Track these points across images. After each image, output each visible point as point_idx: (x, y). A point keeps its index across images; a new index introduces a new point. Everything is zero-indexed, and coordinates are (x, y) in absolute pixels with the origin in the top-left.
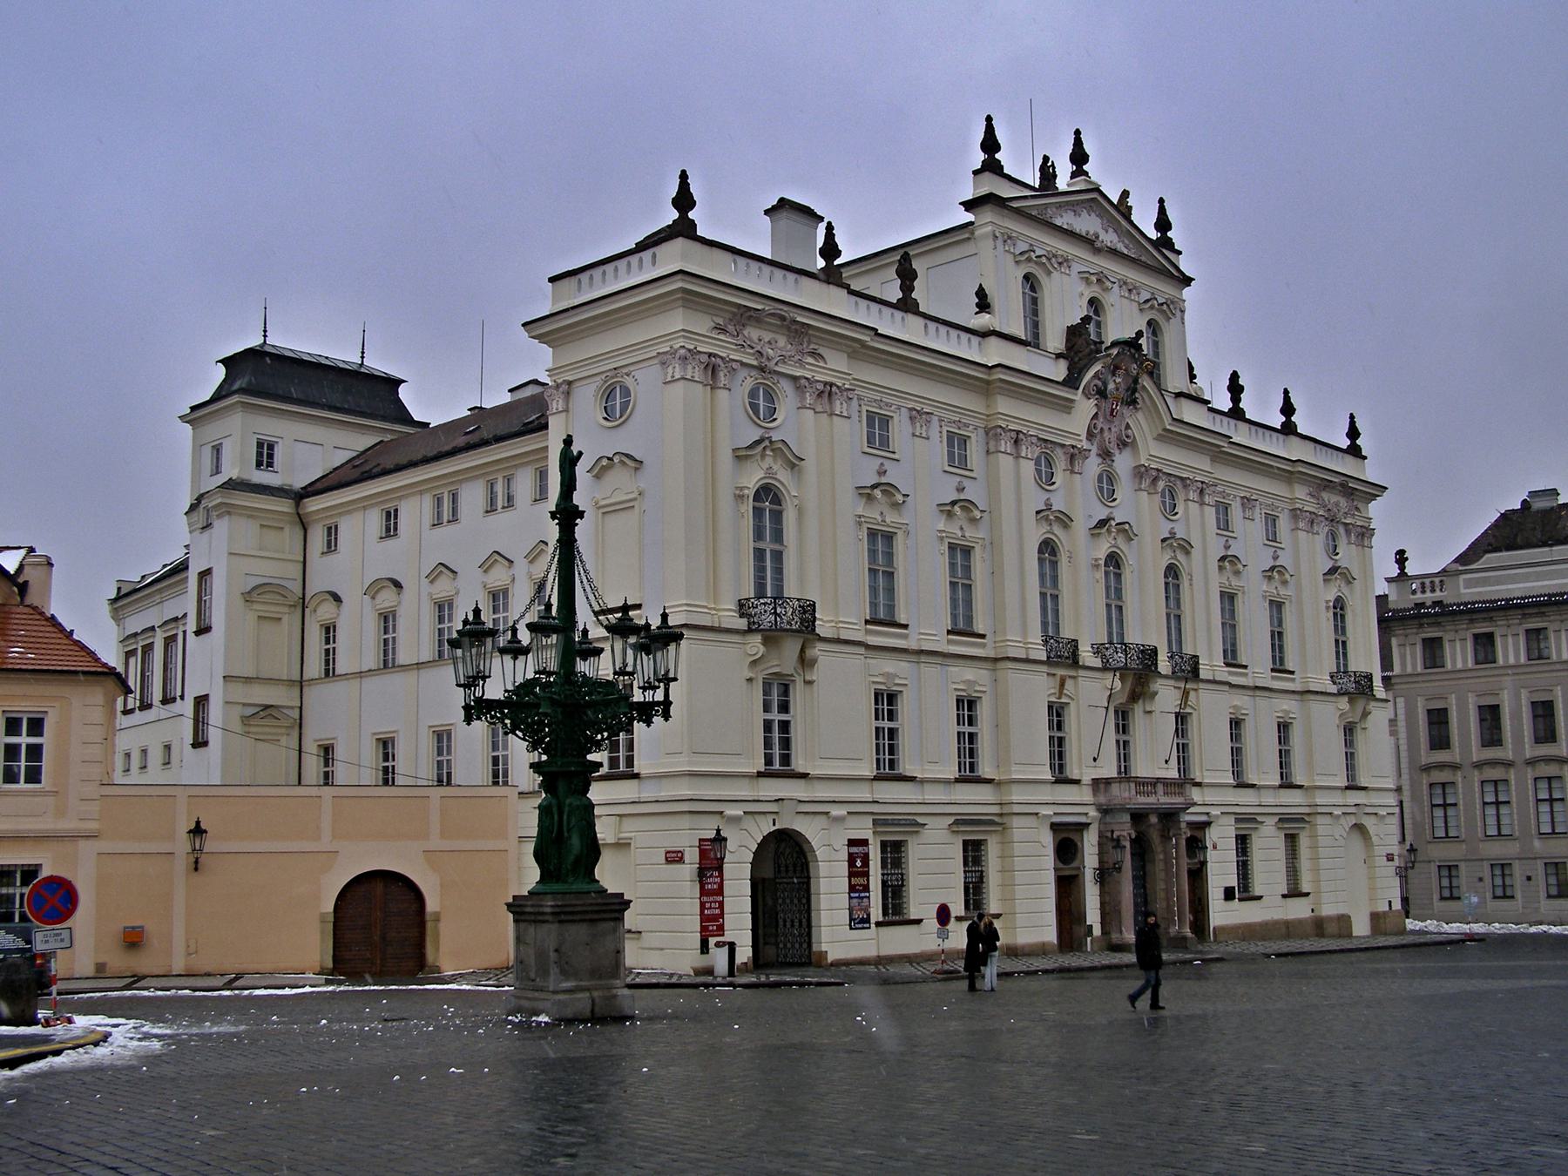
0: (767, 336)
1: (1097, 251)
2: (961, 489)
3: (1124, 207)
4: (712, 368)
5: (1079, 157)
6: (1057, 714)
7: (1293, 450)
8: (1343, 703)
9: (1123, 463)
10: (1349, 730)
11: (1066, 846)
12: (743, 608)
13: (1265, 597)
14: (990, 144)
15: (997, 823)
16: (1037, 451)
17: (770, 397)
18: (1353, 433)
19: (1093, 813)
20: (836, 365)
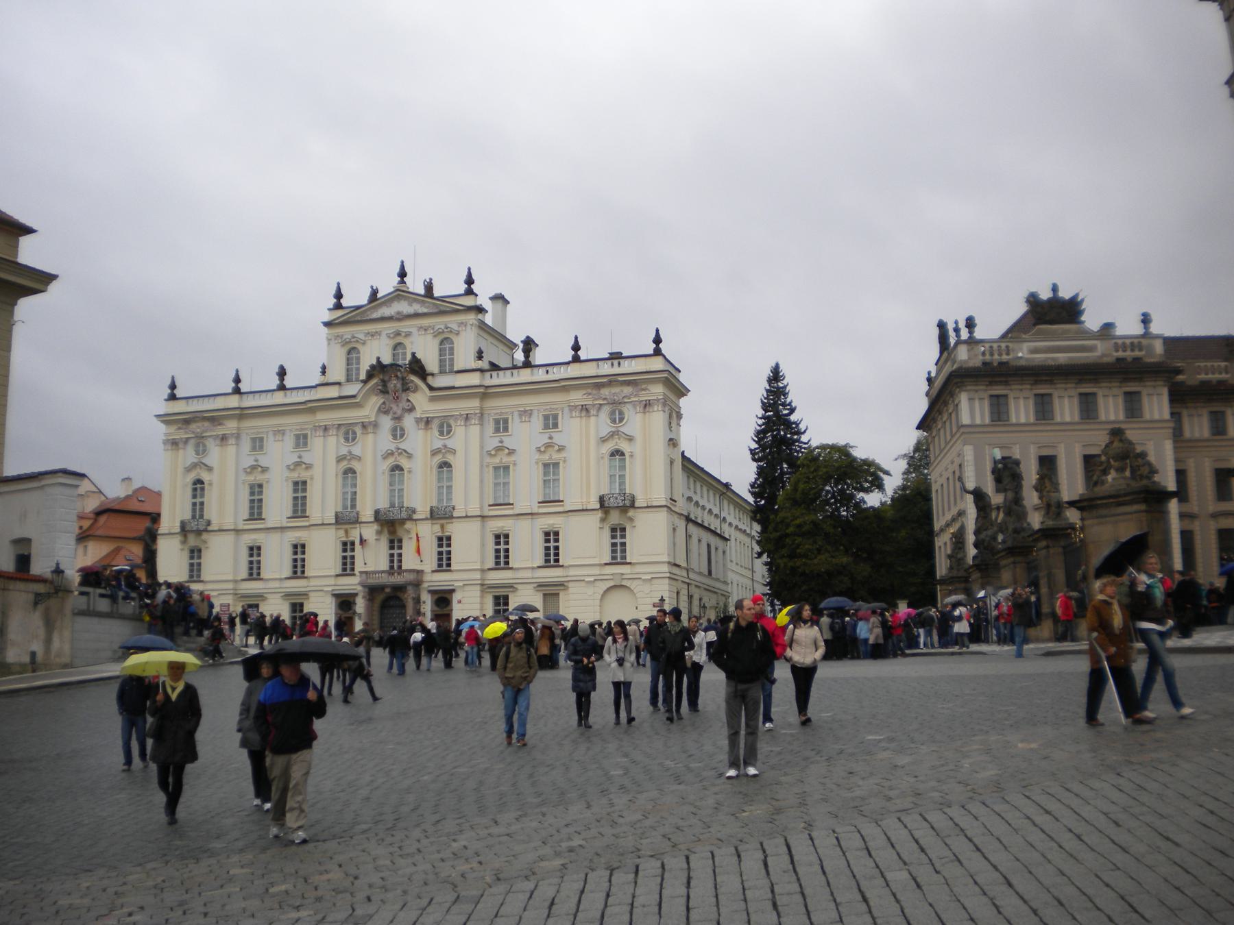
0: (199, 424)
1: (399, 320)
2: (300, 457)
3: (429, 287)
4: (174, 444)
5: (403, 274)
6: (348, 546)
7: (575, 371)
8: (599, 514)
9: (408, 421)
10: (618, 532)
11: (345, 603)
12: (183, 525)
13: (537, 463)
14: (339, 295)
15: (305, 595)
16: (343, 429)
17: (204, 446)
18: (657, 340)
19: (360, 588)
20: (231, 426)
